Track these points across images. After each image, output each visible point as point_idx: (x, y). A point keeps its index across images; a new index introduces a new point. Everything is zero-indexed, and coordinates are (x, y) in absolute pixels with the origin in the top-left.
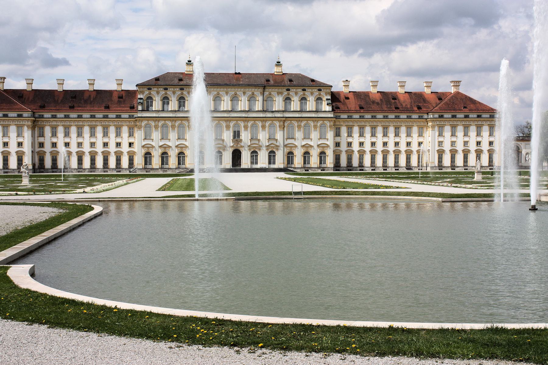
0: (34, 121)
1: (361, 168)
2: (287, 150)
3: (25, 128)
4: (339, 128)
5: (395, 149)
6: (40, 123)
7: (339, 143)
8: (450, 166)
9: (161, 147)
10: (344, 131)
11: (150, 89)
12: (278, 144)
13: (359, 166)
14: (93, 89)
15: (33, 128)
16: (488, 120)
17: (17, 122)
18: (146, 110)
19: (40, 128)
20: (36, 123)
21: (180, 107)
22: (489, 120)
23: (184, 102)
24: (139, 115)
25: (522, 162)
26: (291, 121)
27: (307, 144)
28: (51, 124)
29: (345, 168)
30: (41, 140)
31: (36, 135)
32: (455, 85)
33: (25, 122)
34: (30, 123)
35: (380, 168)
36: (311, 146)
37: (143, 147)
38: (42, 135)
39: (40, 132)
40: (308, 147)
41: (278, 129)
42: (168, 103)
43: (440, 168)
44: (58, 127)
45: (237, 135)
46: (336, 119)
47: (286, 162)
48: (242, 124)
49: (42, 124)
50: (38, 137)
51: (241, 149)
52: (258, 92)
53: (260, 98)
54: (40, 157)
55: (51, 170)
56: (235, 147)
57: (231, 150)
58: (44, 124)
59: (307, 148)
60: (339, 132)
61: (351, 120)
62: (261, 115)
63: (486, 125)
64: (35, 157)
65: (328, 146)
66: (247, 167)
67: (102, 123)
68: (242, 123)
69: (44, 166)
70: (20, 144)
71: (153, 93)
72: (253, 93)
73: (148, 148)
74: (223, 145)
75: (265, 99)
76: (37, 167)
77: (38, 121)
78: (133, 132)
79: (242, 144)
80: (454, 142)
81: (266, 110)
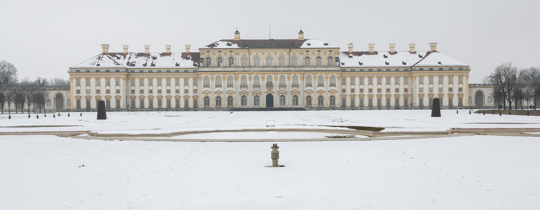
0: (128, 75)
2: (306, 95)
3: (121, 80)
4: (345, 79)
5: (341, 94)
6: (132, 76)
7: (345, 90)
8: (428, 106)
9: (215, 92)
10: (348, 80)
11: (208, 52)
12: (299, 90)
14: (107, 51)
15: (127, 79)
16: (457, 72)
17: (116, 75)
18: (206, 66)
19: (132, 80)
20: (129, 76)
21: (230, 65)
22: (458, 72)
23: (233, 61)
24: (201, 69)
25: (485, 103)
26: (309, 74)
27: (321, 90)
28: (139, 77)
29: (349, 108)
30: (133, 88)
31: (129, 85)
32: (433, 46)
33: (121, 76)
34: (124, 76)
36: (324, 92)
37: (203, 92)
38: (133, 85)
39: (132, 82)
40: (321, 92)
41: (299, 79)
42: (221, 62)
44: (81, 79)
45: (270, 85)
46: (342, 72)
47: (305, 103)
48: (273, 76)
49: (133, 77)
50: (130, 86)
51: (272, 94)
52: (284, 52)
53: (287, 57)
54: (132, 100)
55: (139, 109)
57: (266, 94)
58: (135, 77)
60: (345, 82)
61: (372, 72)
62: (242, 69)
64: (128, 100)
65: (336, 91)
66: (277, 107)
67: (174, 76)
68: (273, 75)
69: (135, 107)
70: (118, 91)
71: (211, 54)
72: (282, 53)
73: (207, 93)
74: (259, 91)
75: (291, 58)
76: (130, 107)
77: (131, 75)
78: (196, 82)
79: (274, 90)
81: (291, 66)
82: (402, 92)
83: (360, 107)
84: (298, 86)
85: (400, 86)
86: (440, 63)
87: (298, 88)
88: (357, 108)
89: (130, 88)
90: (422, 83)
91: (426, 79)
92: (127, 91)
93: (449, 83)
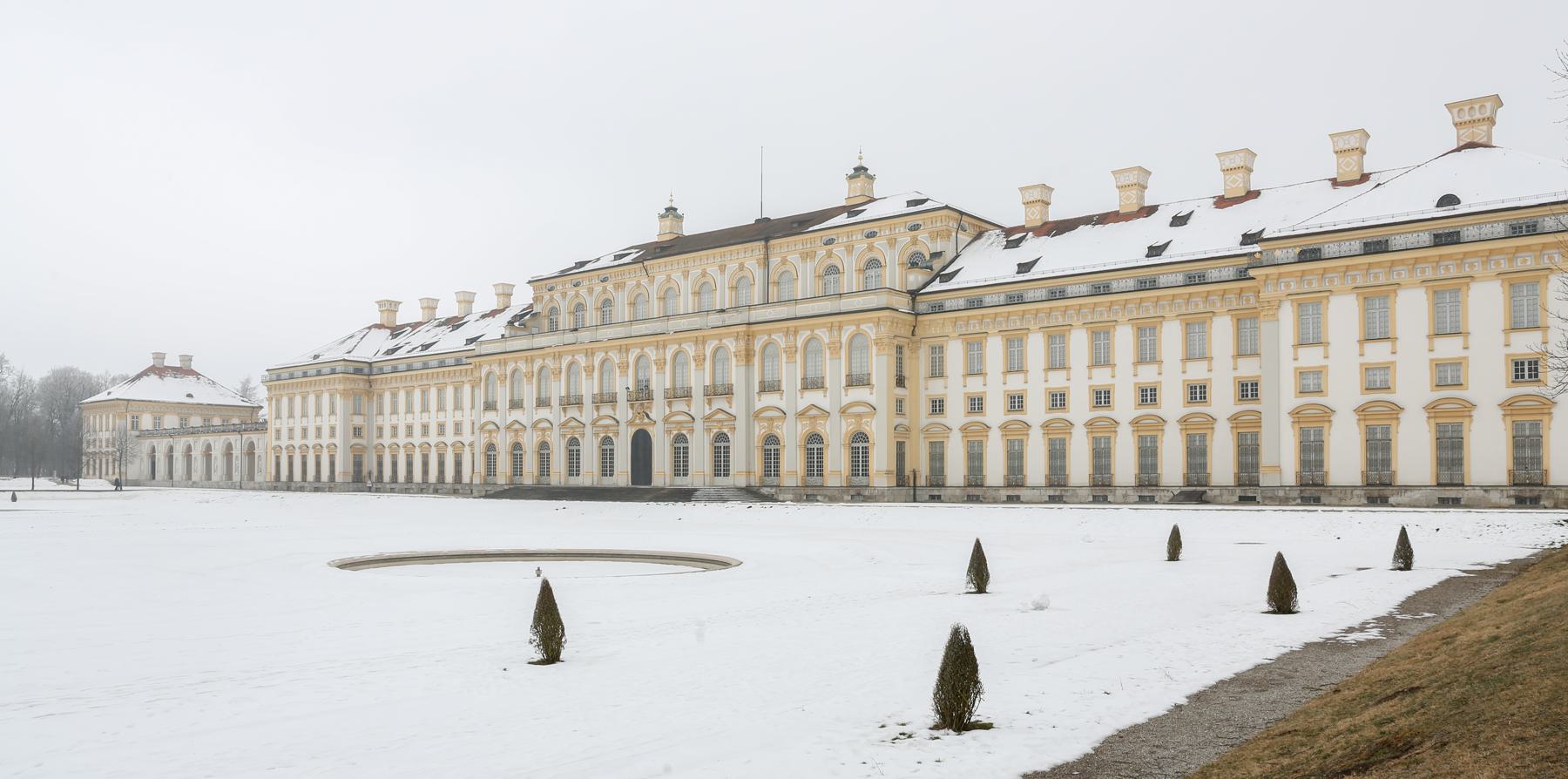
1: (1011, 492)
2: (759, 431)
12: (733, 411)
13: (1009, 485)
29: (958, 492)
35: (1078, 491)
38: (380, 413)
40: (814, 417)
43: (1306, 494)
50: (377, 415)
52: (748, 256)
56: (638, 425)
57: (632, 430)
59: (813, 420)
63: (1485, 279)
70: (333, 429)
80: (1314, 373)
82: (1223, 402)
83: (1009, 485)
84: (728, 392)
85: (1210, 370)
86: (1448, 200)
87: (581, 412)
88: (991, 493)
89: (376, 421)
90: (1310, 337)
91: (1343, 313)
92: (357, 432)
93: (1368, 339)
